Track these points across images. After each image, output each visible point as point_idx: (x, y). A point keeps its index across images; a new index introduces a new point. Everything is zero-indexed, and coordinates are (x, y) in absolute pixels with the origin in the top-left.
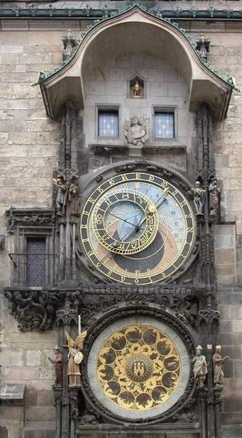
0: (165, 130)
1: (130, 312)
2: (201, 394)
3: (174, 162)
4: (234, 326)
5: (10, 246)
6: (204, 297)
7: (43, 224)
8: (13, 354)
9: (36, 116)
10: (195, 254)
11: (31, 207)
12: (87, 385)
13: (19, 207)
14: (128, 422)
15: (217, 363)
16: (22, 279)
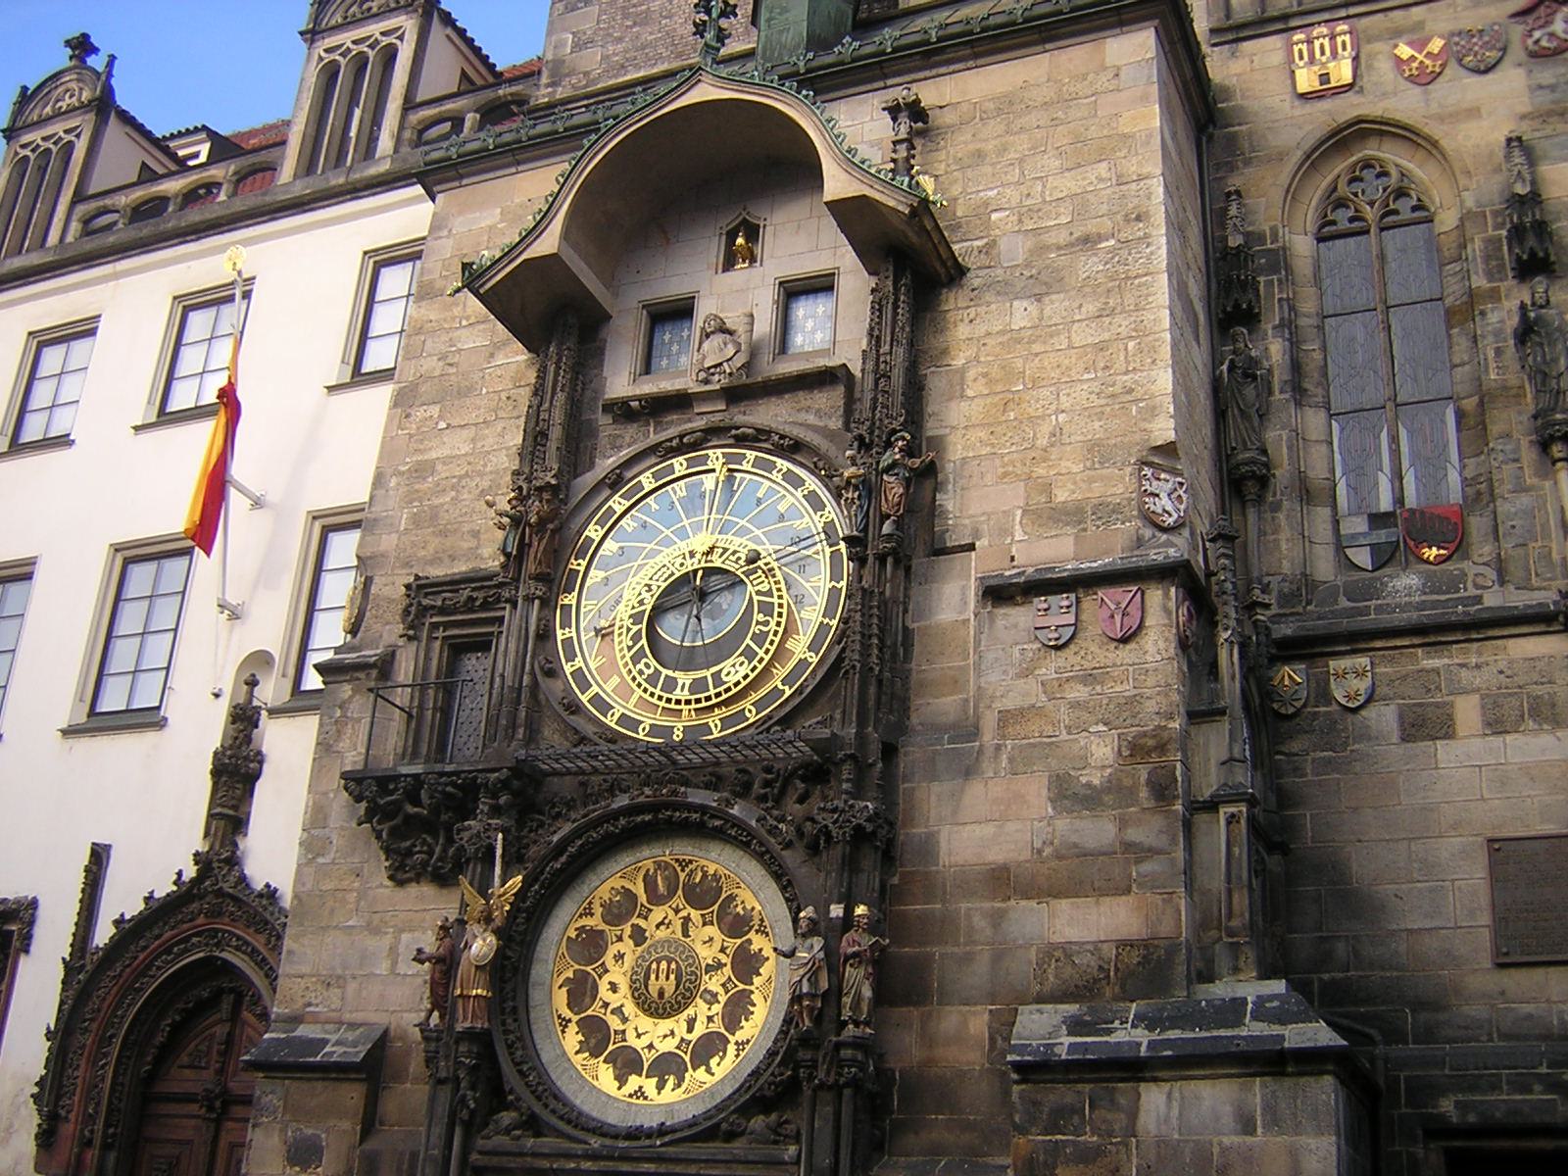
0: (813, 331)
1: (639, 819)
2: (804, 1055)
3: (808, 409)
4: (943, 844)
5: (405, 669)
6: (836, 764)
7: (486, 606)
8: (371, 943)
9: (507, 357)
10: (839, 643)
11: (464, 569)
12: (511, 1025)
13: (437, 572)
14: (604, 1135)
15: (847, 958)
16: (424, 749)
